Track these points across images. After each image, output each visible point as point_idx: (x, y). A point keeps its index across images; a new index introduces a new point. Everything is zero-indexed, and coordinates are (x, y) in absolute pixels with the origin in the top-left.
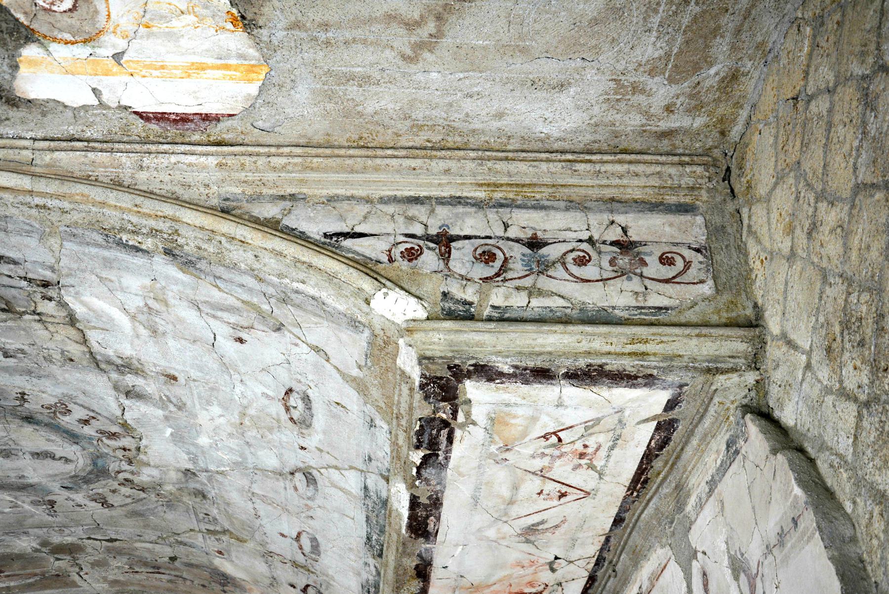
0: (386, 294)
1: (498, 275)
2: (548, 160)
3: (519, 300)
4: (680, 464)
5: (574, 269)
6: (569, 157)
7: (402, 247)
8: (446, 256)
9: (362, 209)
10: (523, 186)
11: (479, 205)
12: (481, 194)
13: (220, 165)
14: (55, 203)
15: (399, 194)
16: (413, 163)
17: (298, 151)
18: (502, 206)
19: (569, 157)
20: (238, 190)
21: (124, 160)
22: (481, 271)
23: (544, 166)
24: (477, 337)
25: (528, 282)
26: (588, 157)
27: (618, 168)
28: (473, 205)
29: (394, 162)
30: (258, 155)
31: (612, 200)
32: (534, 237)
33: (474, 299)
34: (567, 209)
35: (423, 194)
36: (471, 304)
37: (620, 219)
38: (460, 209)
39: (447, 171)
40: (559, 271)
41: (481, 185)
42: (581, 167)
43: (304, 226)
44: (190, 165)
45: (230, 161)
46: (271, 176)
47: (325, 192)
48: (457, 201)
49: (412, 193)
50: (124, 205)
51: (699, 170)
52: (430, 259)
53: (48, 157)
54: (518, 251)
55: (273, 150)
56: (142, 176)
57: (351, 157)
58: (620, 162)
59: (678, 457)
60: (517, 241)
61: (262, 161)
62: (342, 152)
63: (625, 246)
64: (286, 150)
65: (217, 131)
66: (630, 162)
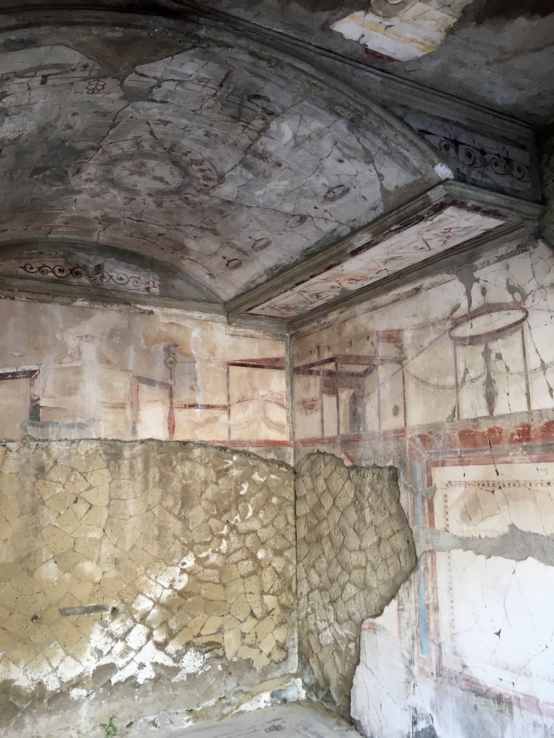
0: (442, 165)
1: (473, 164)
2: (489, 114)
3: (479, 178)
4: (480, 247)
5: (494, 166)
6: (496, 114)
7: (444, 143)
8: (457, 151)
9: (429, 120)
10: (479, 123)
11: (465, 128)
12: (466, 123)
13: (382, 82)
14: (319, 84)
15: (441, 115)
16: (447, 102)
17: (410, 83)
18: (472, 131)
19: (496, 114)
20: (387, 97)
21: (348, 68)
22: (469, 162)
23: (487, 115)
24: (468, 191)
25: (481, 169)
26: (501, 116)
27: (508, 124)
28: (464, 128)
29: (442, 99)
30: (396, 81)
31: (504, 138)
32: (482, 149)
33: (466, 173)
34: (491, 138)
35: (448, 118)
36: (465, 175)
37: (506, 147)
38: (461, 129)
39: (457, 109)
40: (489, 167)
41: (467, 119)
42: (498, 119)
43: (412, 124)
44: (371, 78)
45: (386, 81)
46: (399, 93)
47: (417, 107)
48: (457, 124)
49: (444, 116)
50: (350, 95)
51: (530, 131)
52: (452, 150)
53: (320, 58)
54: (478, 154)
55: (402, 80)
56: (354, 79)
57: (428, 92)
58: (510, 121)
59: (482, 244)
60: (477, 149)
61: (397, 84)
62: (425, 89)
63: (508, 161)
64: (407, 82)
65: (388, 66)
66: (513, 122)
